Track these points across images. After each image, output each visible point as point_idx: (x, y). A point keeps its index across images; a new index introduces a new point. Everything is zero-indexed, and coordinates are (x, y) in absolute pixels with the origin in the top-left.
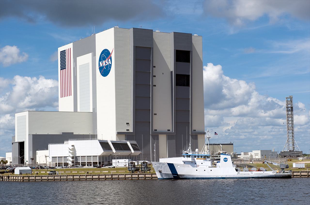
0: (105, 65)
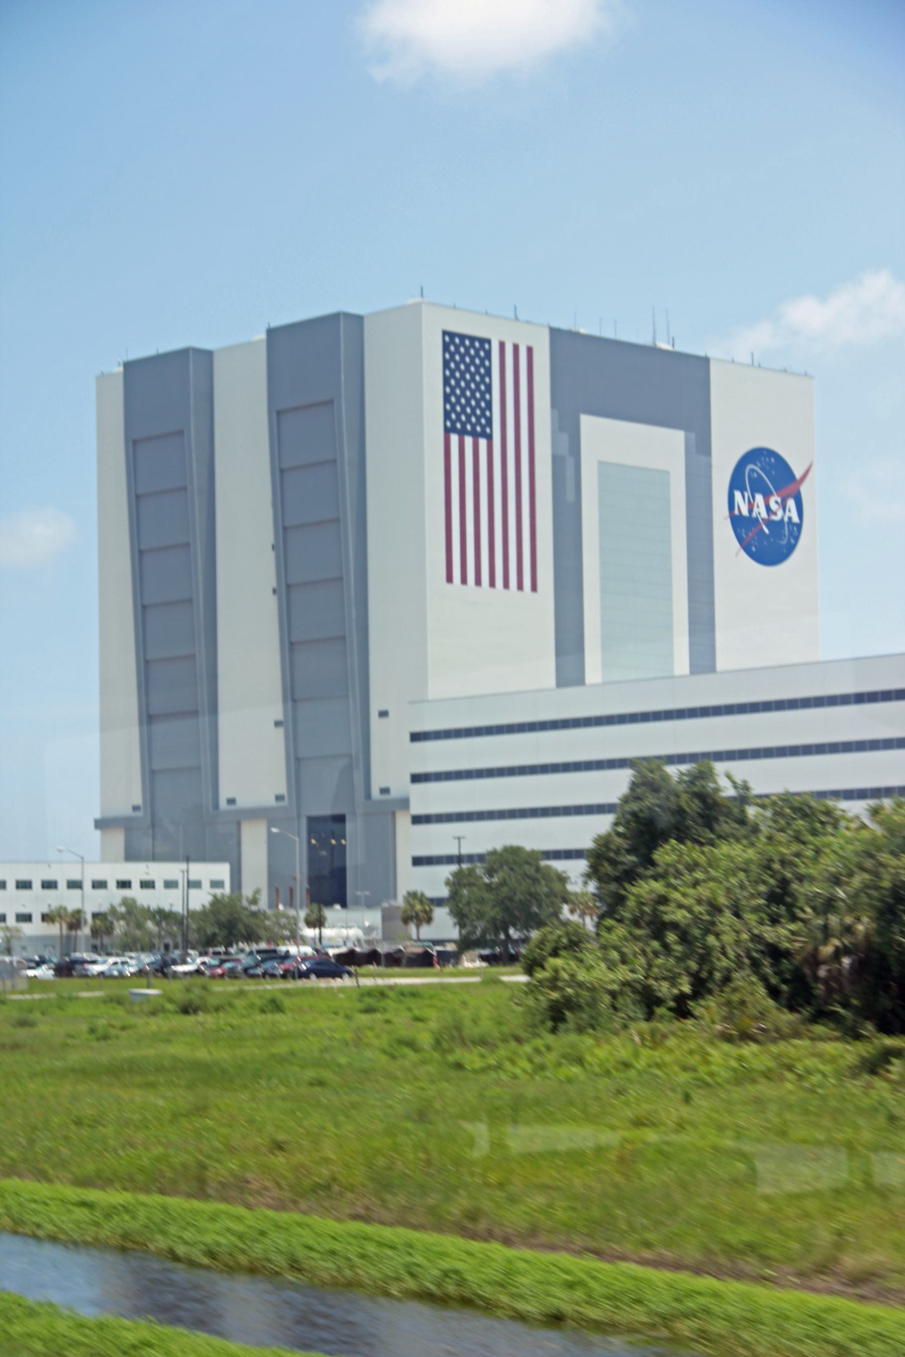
0: (764, 515)
